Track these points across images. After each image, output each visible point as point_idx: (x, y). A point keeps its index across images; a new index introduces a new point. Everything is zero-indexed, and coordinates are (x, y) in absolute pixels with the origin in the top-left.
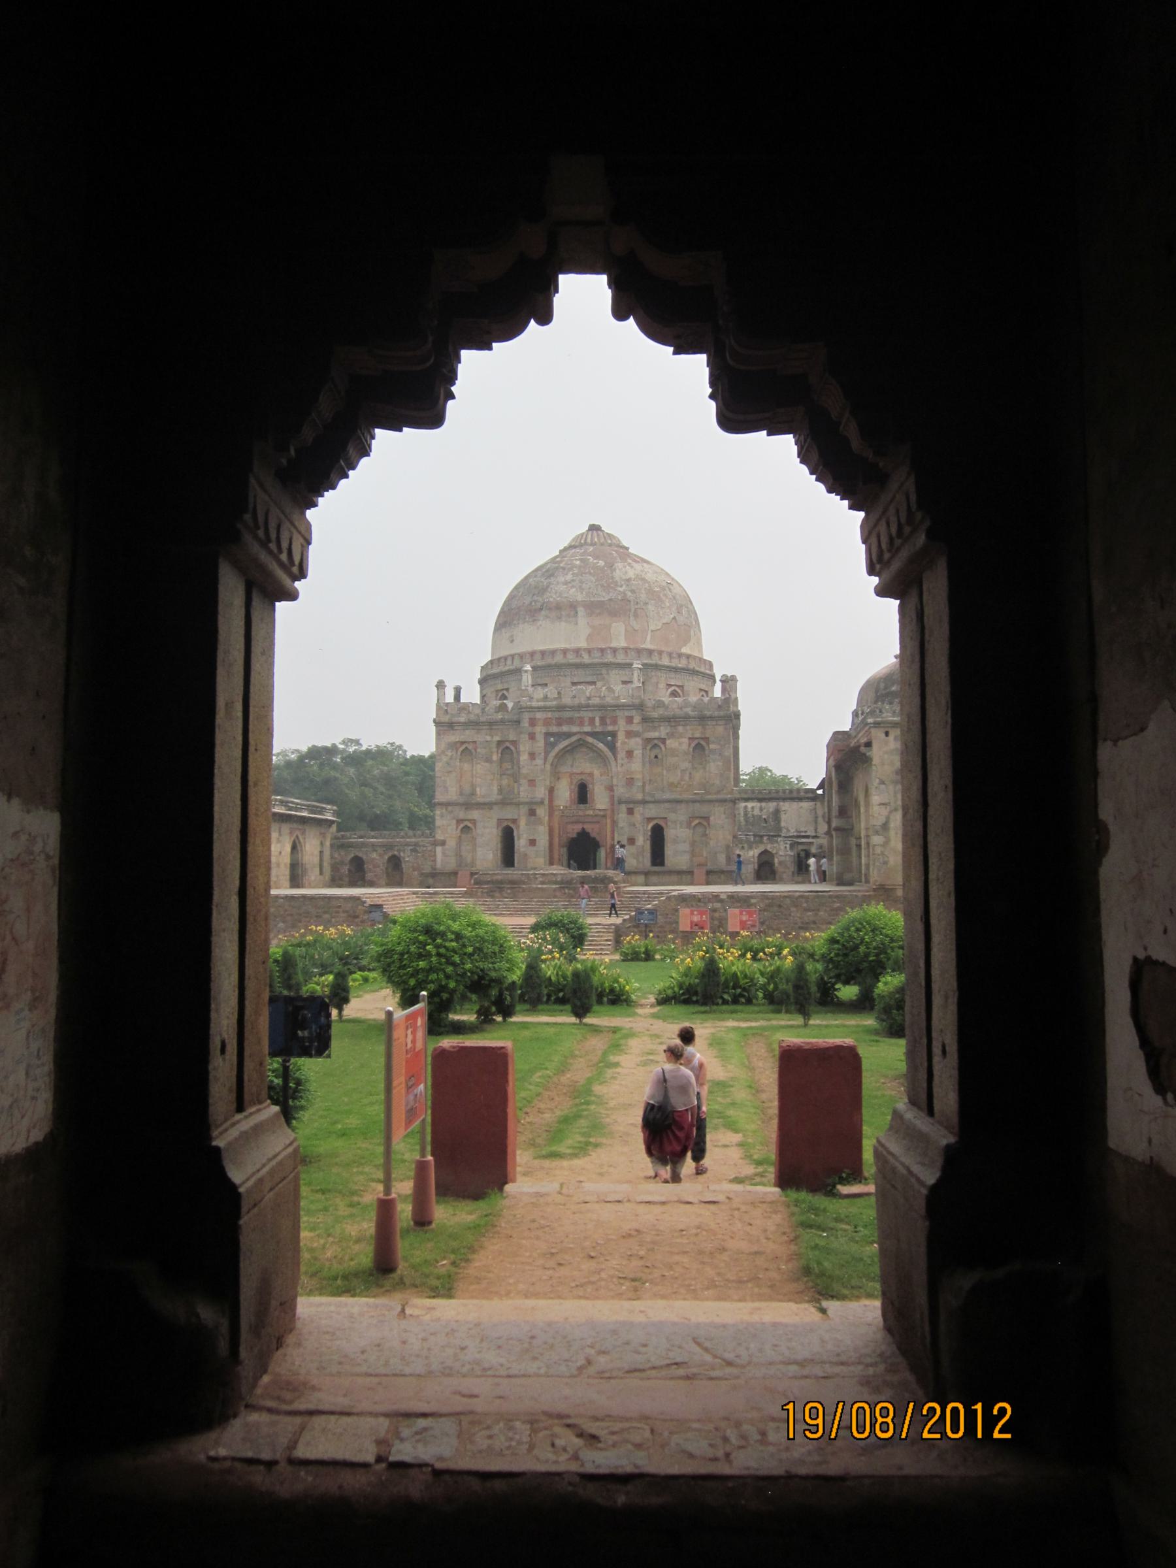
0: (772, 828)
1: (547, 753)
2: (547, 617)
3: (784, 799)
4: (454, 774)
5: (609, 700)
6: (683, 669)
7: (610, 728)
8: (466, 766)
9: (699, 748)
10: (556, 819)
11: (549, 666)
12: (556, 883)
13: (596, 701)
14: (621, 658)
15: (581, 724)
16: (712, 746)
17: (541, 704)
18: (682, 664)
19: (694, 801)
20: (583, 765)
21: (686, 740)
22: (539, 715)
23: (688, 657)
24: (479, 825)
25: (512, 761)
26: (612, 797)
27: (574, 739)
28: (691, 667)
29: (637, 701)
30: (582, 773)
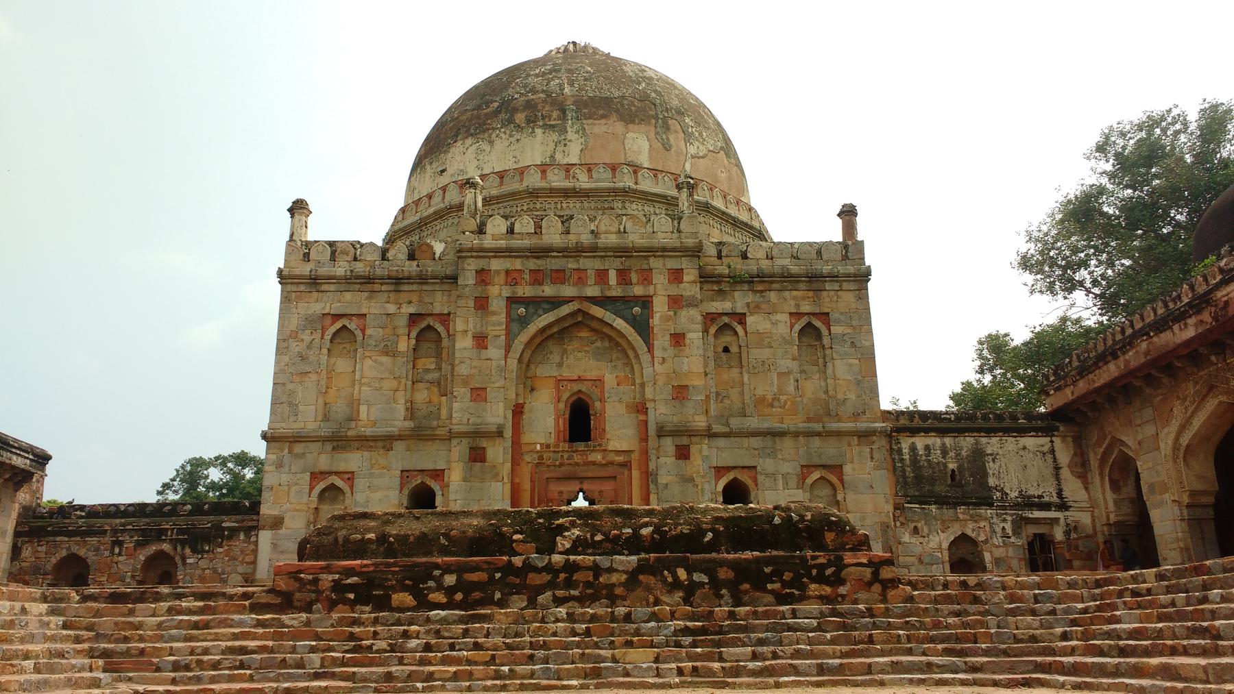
0: (968, 489)
1: (510, 338)
2: (511, 121)
3: (990, 432)
4: (314, 377)
5: (636, 238)
6: (746, 225)
7: (638, 290)
8: (342, 364)
9: (811, 332)
10: (526, 472)
11: (513, 195)
12: (634, 544)
13: (611, 240)
14: (647, 184)
15: (581, 281)
16: (834, 329)
17: (502, 243)
18: (744, 217)
19: (810, 434)
20: (581, 363)
21: (783, 318)
22: (496, 265)
23: (750, 209)
24: (360, 483)
25: (438, 356)
26: (646, 422)
27: (565, 310)
28: (755, 224)
29: (690, 242)
30: (580, 380)
